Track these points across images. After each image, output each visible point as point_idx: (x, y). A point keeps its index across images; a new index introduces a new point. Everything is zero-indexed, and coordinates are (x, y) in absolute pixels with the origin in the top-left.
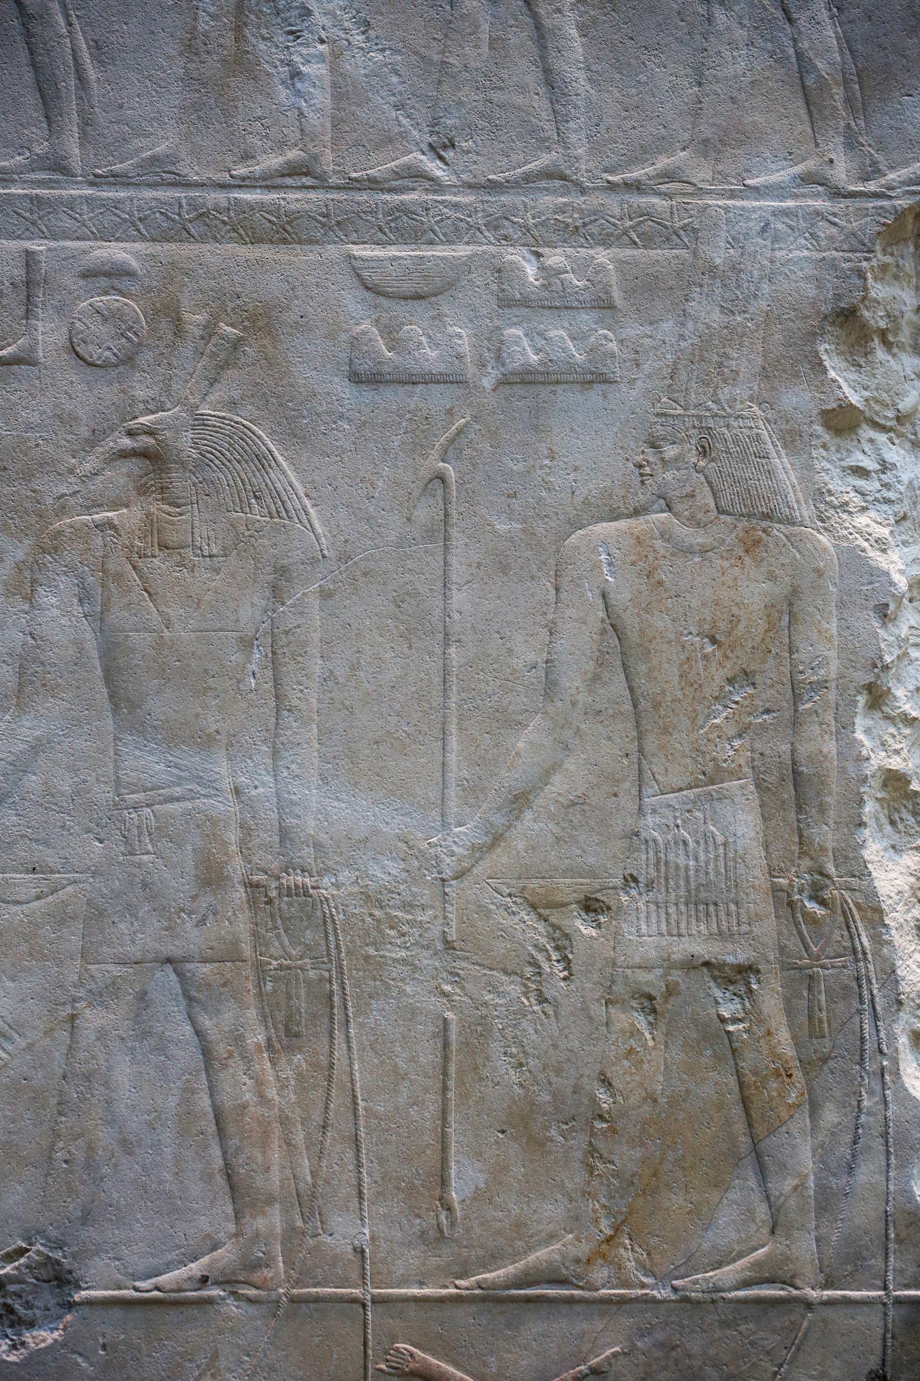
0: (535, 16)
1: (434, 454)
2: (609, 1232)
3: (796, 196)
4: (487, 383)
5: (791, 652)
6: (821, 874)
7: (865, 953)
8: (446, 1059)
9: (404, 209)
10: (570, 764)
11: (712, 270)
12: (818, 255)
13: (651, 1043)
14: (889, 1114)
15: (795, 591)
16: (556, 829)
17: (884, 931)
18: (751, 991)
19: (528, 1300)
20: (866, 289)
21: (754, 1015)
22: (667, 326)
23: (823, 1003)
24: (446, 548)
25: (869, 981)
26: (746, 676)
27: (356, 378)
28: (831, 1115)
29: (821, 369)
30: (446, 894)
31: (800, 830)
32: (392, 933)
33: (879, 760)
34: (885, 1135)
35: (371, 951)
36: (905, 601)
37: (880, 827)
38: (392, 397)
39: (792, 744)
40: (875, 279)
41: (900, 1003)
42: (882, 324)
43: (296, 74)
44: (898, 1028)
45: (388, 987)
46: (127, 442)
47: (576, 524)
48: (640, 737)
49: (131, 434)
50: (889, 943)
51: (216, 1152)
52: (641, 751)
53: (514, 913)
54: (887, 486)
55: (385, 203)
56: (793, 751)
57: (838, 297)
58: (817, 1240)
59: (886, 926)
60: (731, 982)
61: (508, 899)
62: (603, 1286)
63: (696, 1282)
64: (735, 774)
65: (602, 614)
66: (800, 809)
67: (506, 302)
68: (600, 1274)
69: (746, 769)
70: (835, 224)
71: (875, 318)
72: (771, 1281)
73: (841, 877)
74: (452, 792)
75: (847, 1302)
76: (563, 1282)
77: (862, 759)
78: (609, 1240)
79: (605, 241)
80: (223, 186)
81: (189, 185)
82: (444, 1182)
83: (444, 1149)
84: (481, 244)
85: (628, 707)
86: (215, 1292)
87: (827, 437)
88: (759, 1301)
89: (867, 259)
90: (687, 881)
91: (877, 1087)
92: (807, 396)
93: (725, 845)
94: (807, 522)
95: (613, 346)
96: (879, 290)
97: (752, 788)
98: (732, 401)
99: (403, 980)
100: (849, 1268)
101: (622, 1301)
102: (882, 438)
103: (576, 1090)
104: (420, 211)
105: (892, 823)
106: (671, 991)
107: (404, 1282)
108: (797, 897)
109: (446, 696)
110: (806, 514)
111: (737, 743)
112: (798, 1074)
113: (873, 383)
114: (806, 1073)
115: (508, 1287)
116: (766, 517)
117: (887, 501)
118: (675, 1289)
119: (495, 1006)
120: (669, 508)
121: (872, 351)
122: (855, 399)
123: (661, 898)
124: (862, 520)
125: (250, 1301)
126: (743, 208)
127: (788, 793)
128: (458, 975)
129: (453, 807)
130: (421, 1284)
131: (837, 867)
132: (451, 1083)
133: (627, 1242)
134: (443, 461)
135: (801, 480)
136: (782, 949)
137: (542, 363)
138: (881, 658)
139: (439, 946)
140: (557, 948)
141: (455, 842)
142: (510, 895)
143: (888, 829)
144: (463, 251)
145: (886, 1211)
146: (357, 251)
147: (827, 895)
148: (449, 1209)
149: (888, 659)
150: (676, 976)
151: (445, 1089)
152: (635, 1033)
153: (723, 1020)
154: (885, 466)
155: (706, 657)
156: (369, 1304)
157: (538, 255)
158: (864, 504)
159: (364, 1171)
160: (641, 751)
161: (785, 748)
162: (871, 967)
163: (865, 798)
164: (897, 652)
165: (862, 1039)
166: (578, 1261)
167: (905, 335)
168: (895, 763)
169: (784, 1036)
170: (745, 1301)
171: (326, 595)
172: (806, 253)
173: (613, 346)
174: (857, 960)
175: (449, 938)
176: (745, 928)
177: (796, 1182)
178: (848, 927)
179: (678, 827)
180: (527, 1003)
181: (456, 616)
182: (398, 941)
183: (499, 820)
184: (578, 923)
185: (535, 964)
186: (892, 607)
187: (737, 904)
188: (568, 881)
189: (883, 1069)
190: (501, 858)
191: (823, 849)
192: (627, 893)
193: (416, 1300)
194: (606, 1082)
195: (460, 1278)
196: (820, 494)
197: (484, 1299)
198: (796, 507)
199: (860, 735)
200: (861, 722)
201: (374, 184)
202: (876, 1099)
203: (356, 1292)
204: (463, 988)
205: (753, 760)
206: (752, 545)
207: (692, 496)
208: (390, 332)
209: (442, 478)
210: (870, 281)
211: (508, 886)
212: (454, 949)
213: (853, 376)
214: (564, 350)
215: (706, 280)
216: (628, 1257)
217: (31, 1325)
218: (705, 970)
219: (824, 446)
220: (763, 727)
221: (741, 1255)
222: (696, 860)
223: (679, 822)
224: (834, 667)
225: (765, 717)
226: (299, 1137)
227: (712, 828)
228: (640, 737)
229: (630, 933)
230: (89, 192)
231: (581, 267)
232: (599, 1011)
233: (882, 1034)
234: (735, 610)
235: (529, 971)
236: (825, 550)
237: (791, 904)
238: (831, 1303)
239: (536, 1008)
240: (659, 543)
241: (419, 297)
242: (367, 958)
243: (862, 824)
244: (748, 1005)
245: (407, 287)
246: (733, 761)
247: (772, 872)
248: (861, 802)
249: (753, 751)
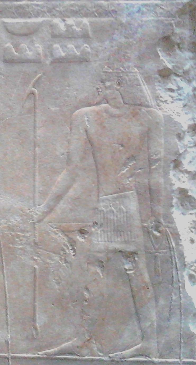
1: (31, 86)
4: (48, 62)
5: (148, 149)
6: (159, 222)
7: (173, 249)
8: (35, 281)
9: (20, 7)
10: (75, 186)
11: (121, 24)
12: (156, 19)
13: (102, 277)
14: (182, 302)
15: (149, 130)
16: (70, 207)
17: (180, 241)
18: (135, 260)
19: (62, 359)
20: (173, 30)
21: (136, 268)
22: (107, 43)
23: (160, 265)
24: (35, 116)
25: (175, 258)
26: (132, 157)
27: (6, 61)
28: (162, 302)
29: (158, 56)
30: (35, 227)
31: (152, 208)
32: (18, 240)
33: (177, 185)
34: (180, 309)
35: (11, 245)
36: (186, 133)
37: (178, 206)
38: (17, 68)
39: (149, 179)
40: (176, 26)
41: (185, 265)
42: (178, 41)
44: (185, 274)
45: (16, 257)
47: (77, 108)
48: (98, 177)
52: (98, 181)
53: (57, 234)
54: (180, 95)
55: (15, 5)
56: (149, 182)
57: (164, 32)
58: (157, 342)
59: (180, 240)
60: (128, 257)
61: (55, 229)
62: (86, 356)
63: (116, 355)
64: (130, 189)
65: (85, 137)
67: (54, 36)
68: (85, 351)
69: (134, 188)
70: (163, 9)
71: (176, 39)
72: (142, 355)
73: (165, 223)
74: (37, 195)
75: (167, 363)
76: (72, 354)
77: (172, 185)
78: (88, 341)
79: (86, 15)
82: (34, 320)
83: (34, 310)
84: (46, 17)
85: (94, 167)
87: (160, 78)
88: (138, 362)
89: (173, 20)
90: (114, 224)
91: (178, 293)
92: (154, 65)
93: (127, 212)
94: (154, 107)
95: (89, 50)
96: (177, 30)
97: (135, 194)
98: (129, 67)
99: (21, 255)
100: (168, 352)
102: (178, 79)
103: (78, 291)
104: (26, 7)
105: (182, 205)
106: (109, 259)
107: (22, 352)
108: (151, 230)
109: (35, 163)
110: (153, 104)
111: (130, 179)
112: (151, 288)
113: (174, 60)
114: (153, 287)
115: (55, 355)
116: (140, 105)
117: (180, 100)
118: (110, 357)
119: (51, 264)
120: (108, 102)
121: (175, 50)
122: (170, 66)
123: (105, 229)
124: (171, 106)
126: (132, 4)
127: (148, 196)
128: (39, 254)
129: (37, 200)
130: (27, 353)
131: (164, 220)
132: (37, 288)
133: (94, 341)
134: (34, 88)
135: (152, 92)
136: (146, 247)
137: (66, 56)
138: (178, 151)
139: (33, 244)
140: (71, 245)
141: (38, 211)
142: (56, 228)
143: (181, 207)
144: (40, 20)
145: (180, 334)
147: (160, 229)
148: (36, 329)
150: (110, 255)
151: (35, 290)
152: (97, 273)
153: (125, 269)
154: (179, 88)
155: (120, 151)
156: (10, 359)
157: (64, 21)
158: (172, 101)
159: (8, 316)
160: (98, 181)
161: (146, 181)
162: (176, 253)
163: (174, 197)
164: (184, 149)
165: (173, 276)
166: (78, 347)
167: (186, 46)
168: (183, 186)
169: (146, 277)
172: (153, 18)
173: (89, 50)
174: (171, 251)
175: (36, 242)
176: (133, 240)
177: (150, 323)
178: (167, 239)
179: (110, 206)
180: (61, 263)
181: (38, 138)
182: (19, 242)
183: (52, 203)
184: (78, 237)
185: (63, 250)
186: (182, 134)
187: (131, 232)
188: (75, 223)
189: (179, 287)
190: (53, 216)
191: (159, 214)
192: (94, 228)
193: (26, 358)
194: (87, 289)
195: (39, 351)
196: (157, 98)
197: (47, 359)
198: (150, 101)
199: (171, 176)
200: (172, 173)
202: (177, 297)
203: (6, 355)
204: (40, 258)
205: (136, 185)
206: (135, 114)
207: (115, 98)
208: (16, 47)
209: (33, 93)
210: (175, 27)
211: (55, 225)
212: (37, 245)
213: (168, 58)
214: (73, 51)
215: (120, 27)
216: (95, 346)
218: (120, 253)
219: (159, 82)
220: (139, 174)
221: (132, 347)
222: (117, 217)
223: (111, 205)
224: (163, 154)
225: (140, 171)
227: (122, 207)
228: (98, 177)
229: (95, 241)
231: (78, 24)
232: (85, 266)
233: (179, 275)
234: (130, 136)
235: (62, 253)
236: (160, 116)
237: (148, 232)
238: (161, 363)
239: (64, 265)
240: (104, 114)
241: (25, 35)
242: (9, 248)
243: (172, 206)
244: (134, 265)
245: (22, 32)
246: (129, 185)
247: (142, 221)
248: (172, 199)
249: (135, 182)
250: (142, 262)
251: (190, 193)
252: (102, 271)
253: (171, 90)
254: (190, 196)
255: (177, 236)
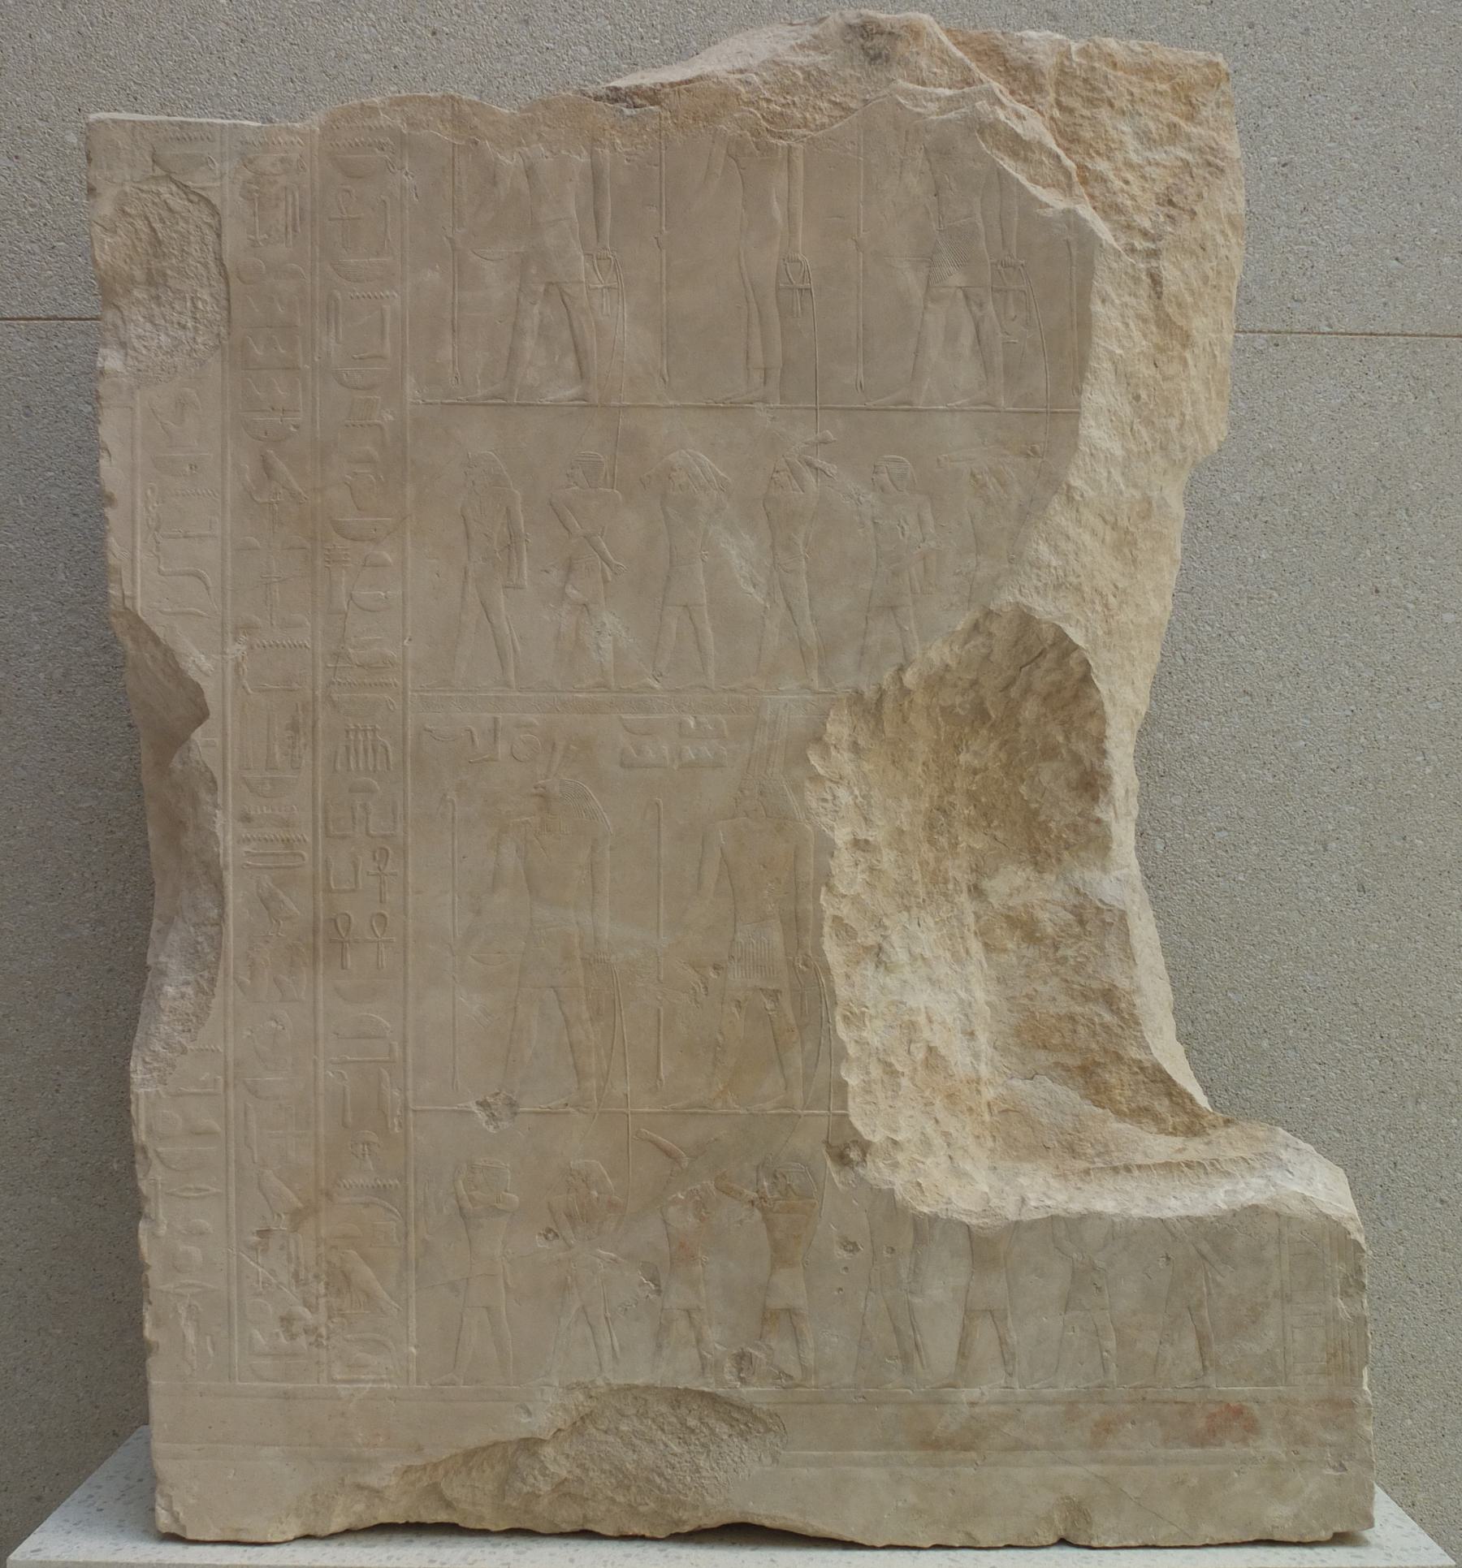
0: (694, 625)
2: (721, 1089)
3: (798, 694)
4: (675, 768)
19: (691, 1114)
27: (622, 765)
28: (809, 1046)
37: (831, 936)
41: (836, 1003)
43: (599, 648)
46: (533, 791)
49: (535, 788)
50: (833, 981)
51: (570, 1059)
56: (795, 909)
66: (798, 931)
76: (705, 1107)
78: (722, 1092)
80: (571, 692)
81: (557, 691)
82: (658, 1070)
86: (571, 1110)
88: (780, 1114)
101: (727, 1114)
105: (837, 936)
112: (796, 1031)
120: (747, 816)
122: (821, 772)
124: (823, 819)
125: (584, 1113)
132: (661, 1033)
146: (623, 716)
149: (834, 873)
151: (659, 1035)
157: (695, 717)
168: (837, 913)
170: (776, 1115)
171: (611, 849)
173: (725, 753)
185: (693, 989)
193: (648, 1113)
199: (822, 902)
201: (630, 690)
203: (624, 1110)
217: (501, 1120)
226: (602, 1053)
230: (518, 694)
235: (692, 992)
237: (794, 966)
248: (822, 928)
250: (786, 1002)
251: (846, 921)
252: (739, 1013)
253: (825, 800)
254: (847, 924)
255: (827, 970)
